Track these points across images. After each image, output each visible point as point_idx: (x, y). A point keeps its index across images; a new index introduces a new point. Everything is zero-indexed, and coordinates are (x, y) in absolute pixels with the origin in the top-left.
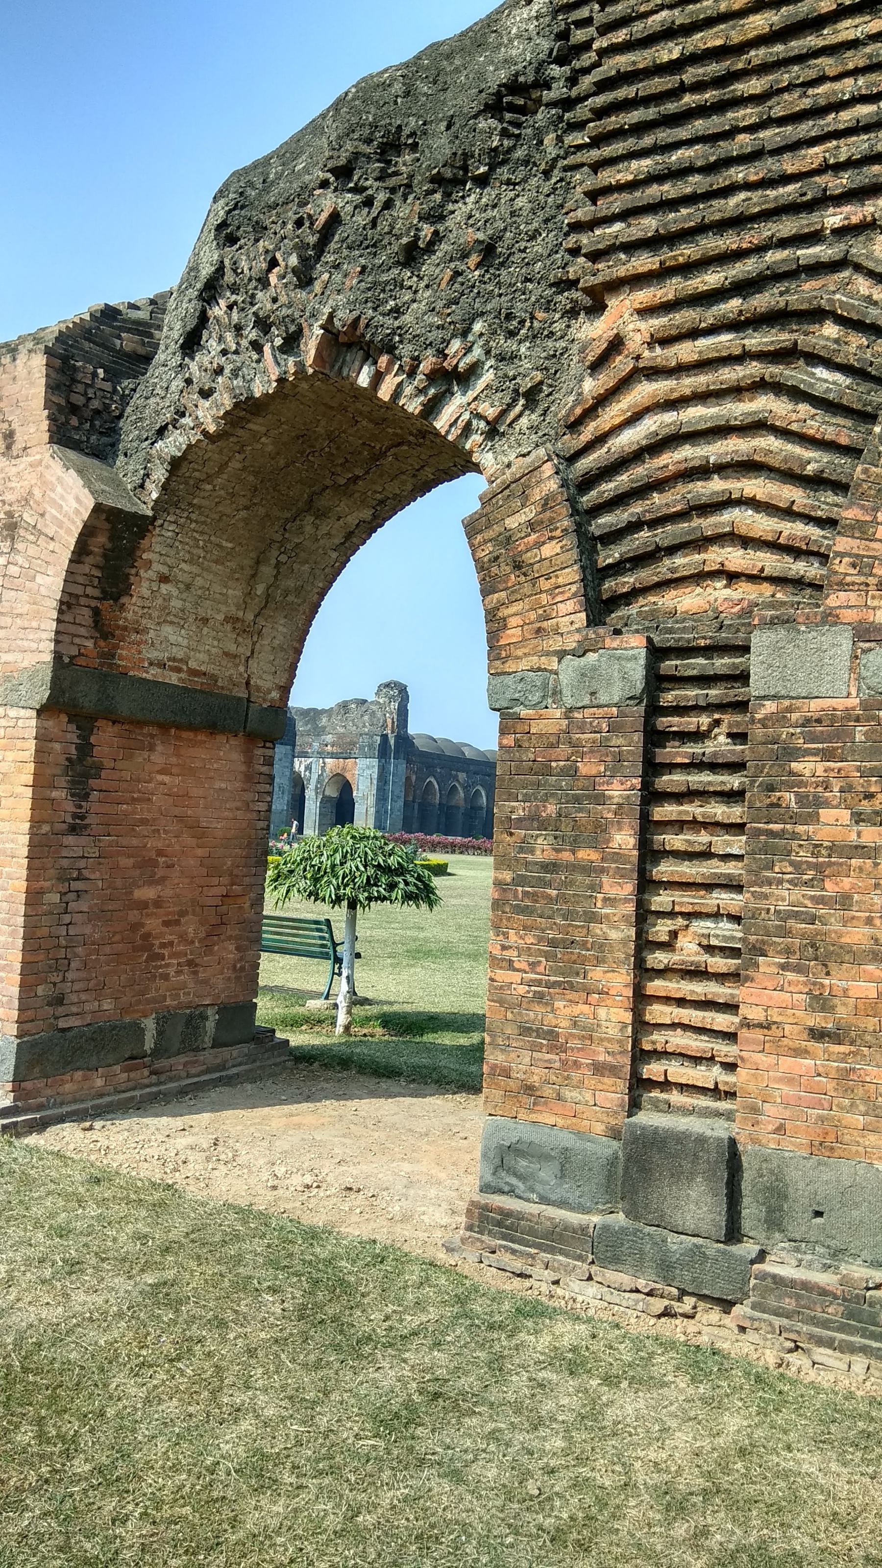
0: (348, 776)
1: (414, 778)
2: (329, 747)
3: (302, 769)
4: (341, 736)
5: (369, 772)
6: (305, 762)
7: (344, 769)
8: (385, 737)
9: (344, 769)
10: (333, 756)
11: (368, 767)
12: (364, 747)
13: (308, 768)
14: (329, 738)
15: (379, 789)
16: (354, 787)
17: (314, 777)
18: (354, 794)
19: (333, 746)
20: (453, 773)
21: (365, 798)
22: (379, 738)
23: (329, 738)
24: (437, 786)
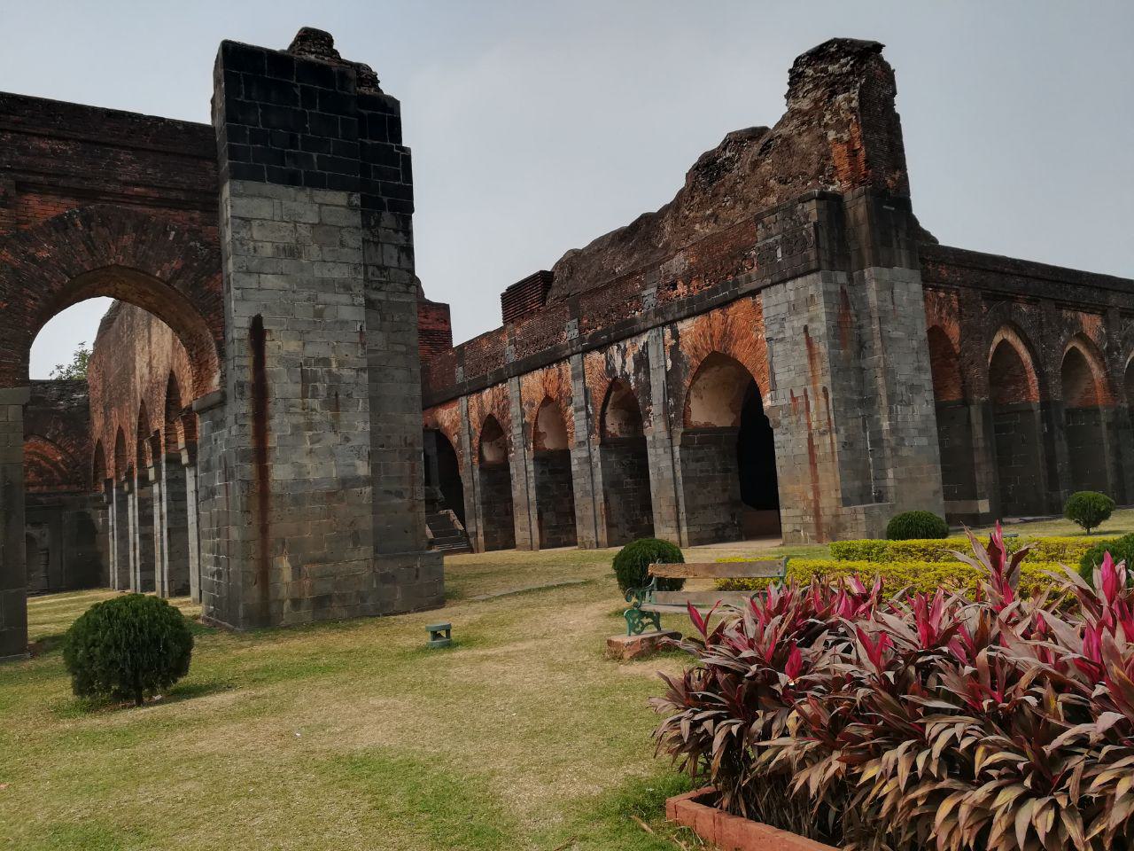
0: (740, 352)
1: (954, 330)
2: (681, 288)
3: (630, 367)
4: (706, 246)
5: (798, 322)
6: (633, 346)
7: (727, 336)
8: (833, 204)
9: (727, 336)
10: (697, 308)
11: (794, 309)
12: (772, 249)
13: (642, 361)
14: (679, 263)
15: (839, 370)
16: (763, 382)
17: (658, 381)
18: (767, 403)
19: (687, 283)
20: (1067, 314)
21: (799, 405)
22: (812, 208)
23: (679, 263)
24: (1025, 355)
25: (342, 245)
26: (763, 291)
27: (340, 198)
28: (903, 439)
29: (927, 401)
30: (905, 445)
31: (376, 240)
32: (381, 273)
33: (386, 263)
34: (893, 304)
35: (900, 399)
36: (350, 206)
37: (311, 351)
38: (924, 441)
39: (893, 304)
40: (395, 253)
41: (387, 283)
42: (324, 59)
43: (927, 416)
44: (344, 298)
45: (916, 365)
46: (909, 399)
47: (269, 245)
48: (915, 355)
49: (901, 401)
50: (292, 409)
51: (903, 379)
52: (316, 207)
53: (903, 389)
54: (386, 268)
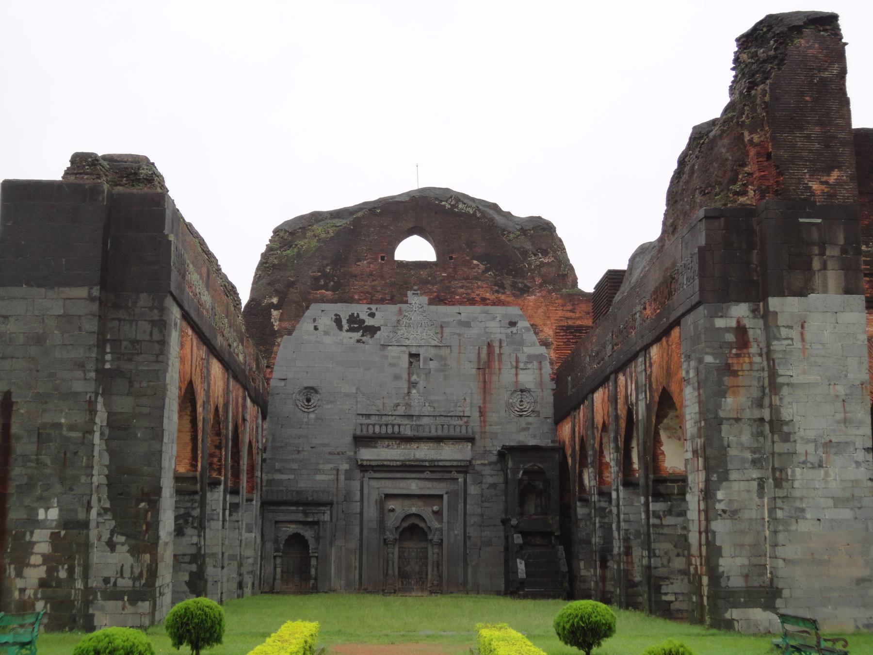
25: (80, 329)
26: (682, 321)
27: (81, 292)
28: (802, 510)
29: (857, 462)
30: (804, 518)
31: (132, 318)
32: (134, 346)
33: (138, 338)
34: (803, 340)
35: (803, 458)
36: (91, 299)
37: (48, 418)
38: (846, 514)
39: (803, 340)
40: (147, 326)
41: (138, 354)
42: (82, 178)
43: (856, 483)
44: (79, 374)
45: (840, 416)
46: (821, 461)
47: (21, 336)
48: (839, 405)
49: (804, 463)
50: (29, 464)
51: (811, 434)
52: (61, 303)
53: (811, 448)
54: (138, 342)
